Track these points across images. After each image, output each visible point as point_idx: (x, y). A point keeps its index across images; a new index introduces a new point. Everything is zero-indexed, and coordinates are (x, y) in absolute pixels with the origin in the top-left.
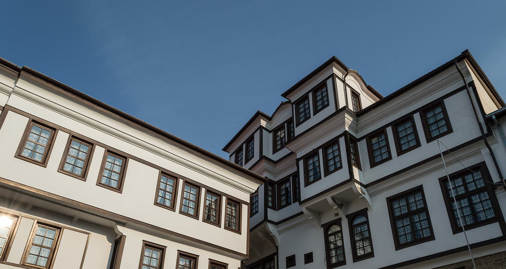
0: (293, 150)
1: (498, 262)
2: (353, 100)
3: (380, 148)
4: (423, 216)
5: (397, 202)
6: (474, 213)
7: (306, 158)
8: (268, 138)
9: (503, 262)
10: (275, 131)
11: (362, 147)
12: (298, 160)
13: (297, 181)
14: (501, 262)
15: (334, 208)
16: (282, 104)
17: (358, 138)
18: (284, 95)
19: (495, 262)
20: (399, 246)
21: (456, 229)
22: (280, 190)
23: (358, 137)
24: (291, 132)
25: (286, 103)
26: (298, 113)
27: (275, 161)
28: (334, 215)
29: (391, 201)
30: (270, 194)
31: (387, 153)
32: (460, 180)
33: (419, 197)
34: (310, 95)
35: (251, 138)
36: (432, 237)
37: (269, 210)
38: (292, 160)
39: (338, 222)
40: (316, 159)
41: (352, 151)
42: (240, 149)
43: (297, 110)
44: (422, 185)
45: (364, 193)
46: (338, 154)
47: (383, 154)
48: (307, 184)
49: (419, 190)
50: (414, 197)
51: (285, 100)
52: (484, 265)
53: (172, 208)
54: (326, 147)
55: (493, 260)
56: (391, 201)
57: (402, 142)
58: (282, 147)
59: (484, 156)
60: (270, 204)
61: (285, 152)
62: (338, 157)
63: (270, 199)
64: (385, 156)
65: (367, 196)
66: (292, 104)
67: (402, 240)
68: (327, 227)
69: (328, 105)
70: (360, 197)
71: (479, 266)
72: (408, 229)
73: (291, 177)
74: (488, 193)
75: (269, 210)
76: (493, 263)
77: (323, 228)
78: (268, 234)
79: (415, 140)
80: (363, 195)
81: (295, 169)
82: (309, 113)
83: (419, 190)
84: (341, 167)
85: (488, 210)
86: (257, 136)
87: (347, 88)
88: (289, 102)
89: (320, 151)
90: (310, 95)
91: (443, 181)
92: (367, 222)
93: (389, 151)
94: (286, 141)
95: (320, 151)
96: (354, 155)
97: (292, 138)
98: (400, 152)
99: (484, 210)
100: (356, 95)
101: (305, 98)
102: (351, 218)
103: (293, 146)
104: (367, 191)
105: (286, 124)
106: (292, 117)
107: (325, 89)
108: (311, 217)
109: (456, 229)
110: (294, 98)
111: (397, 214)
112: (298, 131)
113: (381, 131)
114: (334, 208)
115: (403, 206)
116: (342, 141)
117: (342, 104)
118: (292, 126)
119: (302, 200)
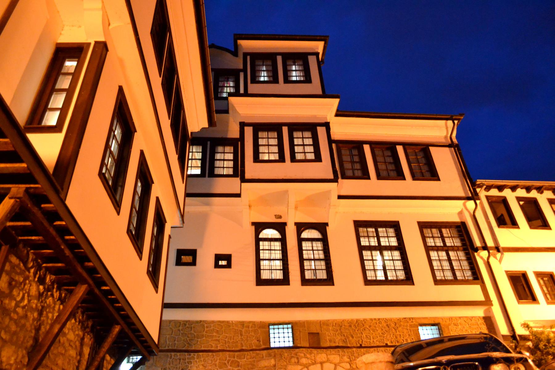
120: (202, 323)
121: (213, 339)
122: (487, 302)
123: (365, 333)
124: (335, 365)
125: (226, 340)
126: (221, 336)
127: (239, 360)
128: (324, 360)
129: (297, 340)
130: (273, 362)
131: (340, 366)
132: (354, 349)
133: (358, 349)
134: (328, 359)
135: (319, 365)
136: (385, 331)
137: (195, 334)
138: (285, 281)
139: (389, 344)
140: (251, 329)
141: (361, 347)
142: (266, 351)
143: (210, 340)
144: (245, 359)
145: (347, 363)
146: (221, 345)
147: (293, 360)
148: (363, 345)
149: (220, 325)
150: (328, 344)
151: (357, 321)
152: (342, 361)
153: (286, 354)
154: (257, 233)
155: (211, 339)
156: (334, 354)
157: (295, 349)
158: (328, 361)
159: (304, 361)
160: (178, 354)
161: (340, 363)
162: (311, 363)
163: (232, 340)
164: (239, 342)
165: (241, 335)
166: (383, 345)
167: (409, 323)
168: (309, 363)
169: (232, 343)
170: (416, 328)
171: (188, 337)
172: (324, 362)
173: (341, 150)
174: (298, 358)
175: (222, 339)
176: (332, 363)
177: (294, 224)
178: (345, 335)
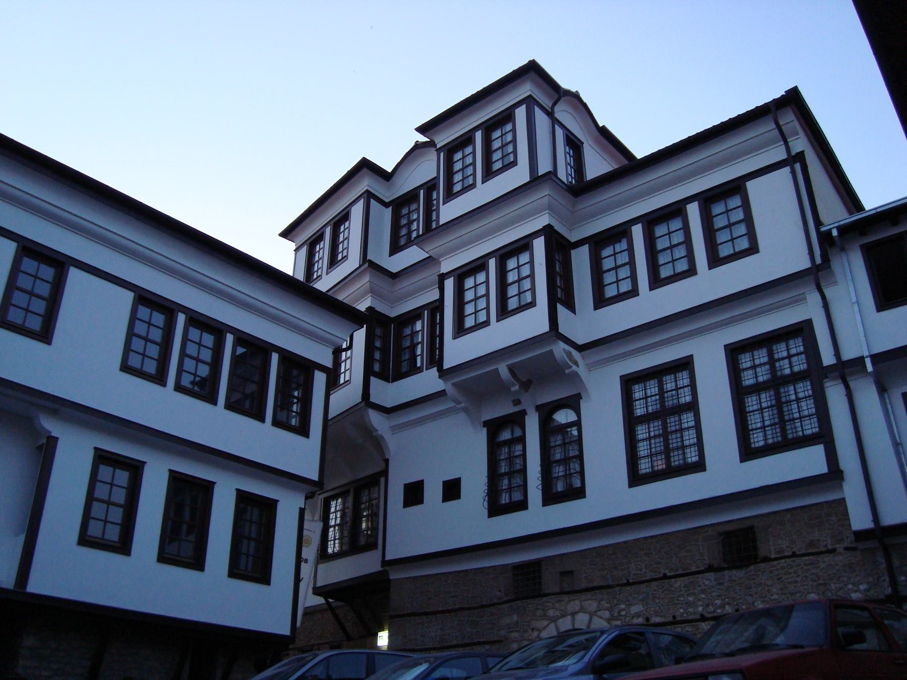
0: (431, 253)
2: (570, 165)
3: (616, 268)
4: (688, 419)
5: (642, 385)
6: (782, 422)
7: (462, 274)
8: (383, 218)
10: (400, 204)
11: (581, 259)
12: (442, 278)
13: (438, 321)
15: (512, 389)
16: (418, 146)
17: (572, 241)
18: (422, 129)
20: (636, 479)
21: (748, 453)
22: (399, 338)
23: (573, 238)
24: (430, 210)
25: (424, 145)
26: (449, 173)
27: (394, 270)
28: (512, 403)
29: (628, 382)
30: (378, 344)
31: (629, 279)
32: (763, 352)
33: (683, 379)
34: (479, 135)
35: (344, 217)
36: (699, 466)
37: (372, 379)
38: (430, 275)
39: (518, 419)
40: (481, 277)
41: (558, 269)
42: (318, 238)
43: (449, 163)
44: (691, 356)
45: (576, 364)
46: (528, 273)
47: (622, 281)
48: (460, 330)
49: (686, 364)
50: (676, 378)
51: (423, 139)
53: (159, 378)
54: (505, 254)
56: (628, 382)
57: (661, 261)
58: (409, 243)
60: (377, 367)
61: (413, 255)
62: (528, 280)
63: (377, 355)
64: (625, 287)
65: (582, 370)
66: (439, 151)
67: (644, 467)
68: (494, 427)
69: (514, 163)
70: (567, 371)
72: (658, 445)
73: (426, 312)
74: (812, 384)
75: (373, 380)
78: (368, 432)
79: (686, 258)
80: (574, 368)
81: (434, 295)
82: (474, 174)
83: (686, 364)
84: (532, 304)
85: (808, 418)
86: (357, 212)
87: (557, 128)
88: (431, 144)
89: (492, 263)
90: (479, 135)
91: (734, 351)
92: (578, 424)
93: (633, 277)
94: (421, 233)
95: (492, 263)
96: (561, 276)
97: (431, 229)
98: (656, 282)
99: (800, 418)
100: (574, 144)
101: (466, 140)
102: (546, 412)
103: (434, 247)
104: (583, 358)
105: (422, 192)
106: (436, 179)
107: (509, 127)
108: (463, 405)
109: (748, 453)
110: (444, 138)
111: (639, 411)
112: (448, 212)
113: (621, 232)
114: (512, 389)
115: (651, 396)
116: (539, 245)
117: (544, 167)
118: (435, 196)
119: (446, 366)
122: (835, 474)
124: (592, 615)
125: (465, 594)
127: (478, 619)
128: (577, 609)
130: (515, 617)
131: (598, 616)
132: (617, 589)
133: (623, 588)
134: (582, 607)
135: (569, 617)
139: (669, 574)
141: (628, 584)
142: (508, 605)
144: (485, 618)
145: (606, 610)
147: (539, 613)
148: (631, 581)
150: (583, 585)
151: (625, 542)
152: (599, 608)
153: (530, 606)
156: (590, 600)
157: (541, 598)
158: (582, 610)
159: (551, 613)
160: (417, 618)
161: (596, 612)
162: (560, 615)
168: (558, 616)
172: (576, 613)
174: (543, 610)
176: (586, 613)
177: (535, 412)
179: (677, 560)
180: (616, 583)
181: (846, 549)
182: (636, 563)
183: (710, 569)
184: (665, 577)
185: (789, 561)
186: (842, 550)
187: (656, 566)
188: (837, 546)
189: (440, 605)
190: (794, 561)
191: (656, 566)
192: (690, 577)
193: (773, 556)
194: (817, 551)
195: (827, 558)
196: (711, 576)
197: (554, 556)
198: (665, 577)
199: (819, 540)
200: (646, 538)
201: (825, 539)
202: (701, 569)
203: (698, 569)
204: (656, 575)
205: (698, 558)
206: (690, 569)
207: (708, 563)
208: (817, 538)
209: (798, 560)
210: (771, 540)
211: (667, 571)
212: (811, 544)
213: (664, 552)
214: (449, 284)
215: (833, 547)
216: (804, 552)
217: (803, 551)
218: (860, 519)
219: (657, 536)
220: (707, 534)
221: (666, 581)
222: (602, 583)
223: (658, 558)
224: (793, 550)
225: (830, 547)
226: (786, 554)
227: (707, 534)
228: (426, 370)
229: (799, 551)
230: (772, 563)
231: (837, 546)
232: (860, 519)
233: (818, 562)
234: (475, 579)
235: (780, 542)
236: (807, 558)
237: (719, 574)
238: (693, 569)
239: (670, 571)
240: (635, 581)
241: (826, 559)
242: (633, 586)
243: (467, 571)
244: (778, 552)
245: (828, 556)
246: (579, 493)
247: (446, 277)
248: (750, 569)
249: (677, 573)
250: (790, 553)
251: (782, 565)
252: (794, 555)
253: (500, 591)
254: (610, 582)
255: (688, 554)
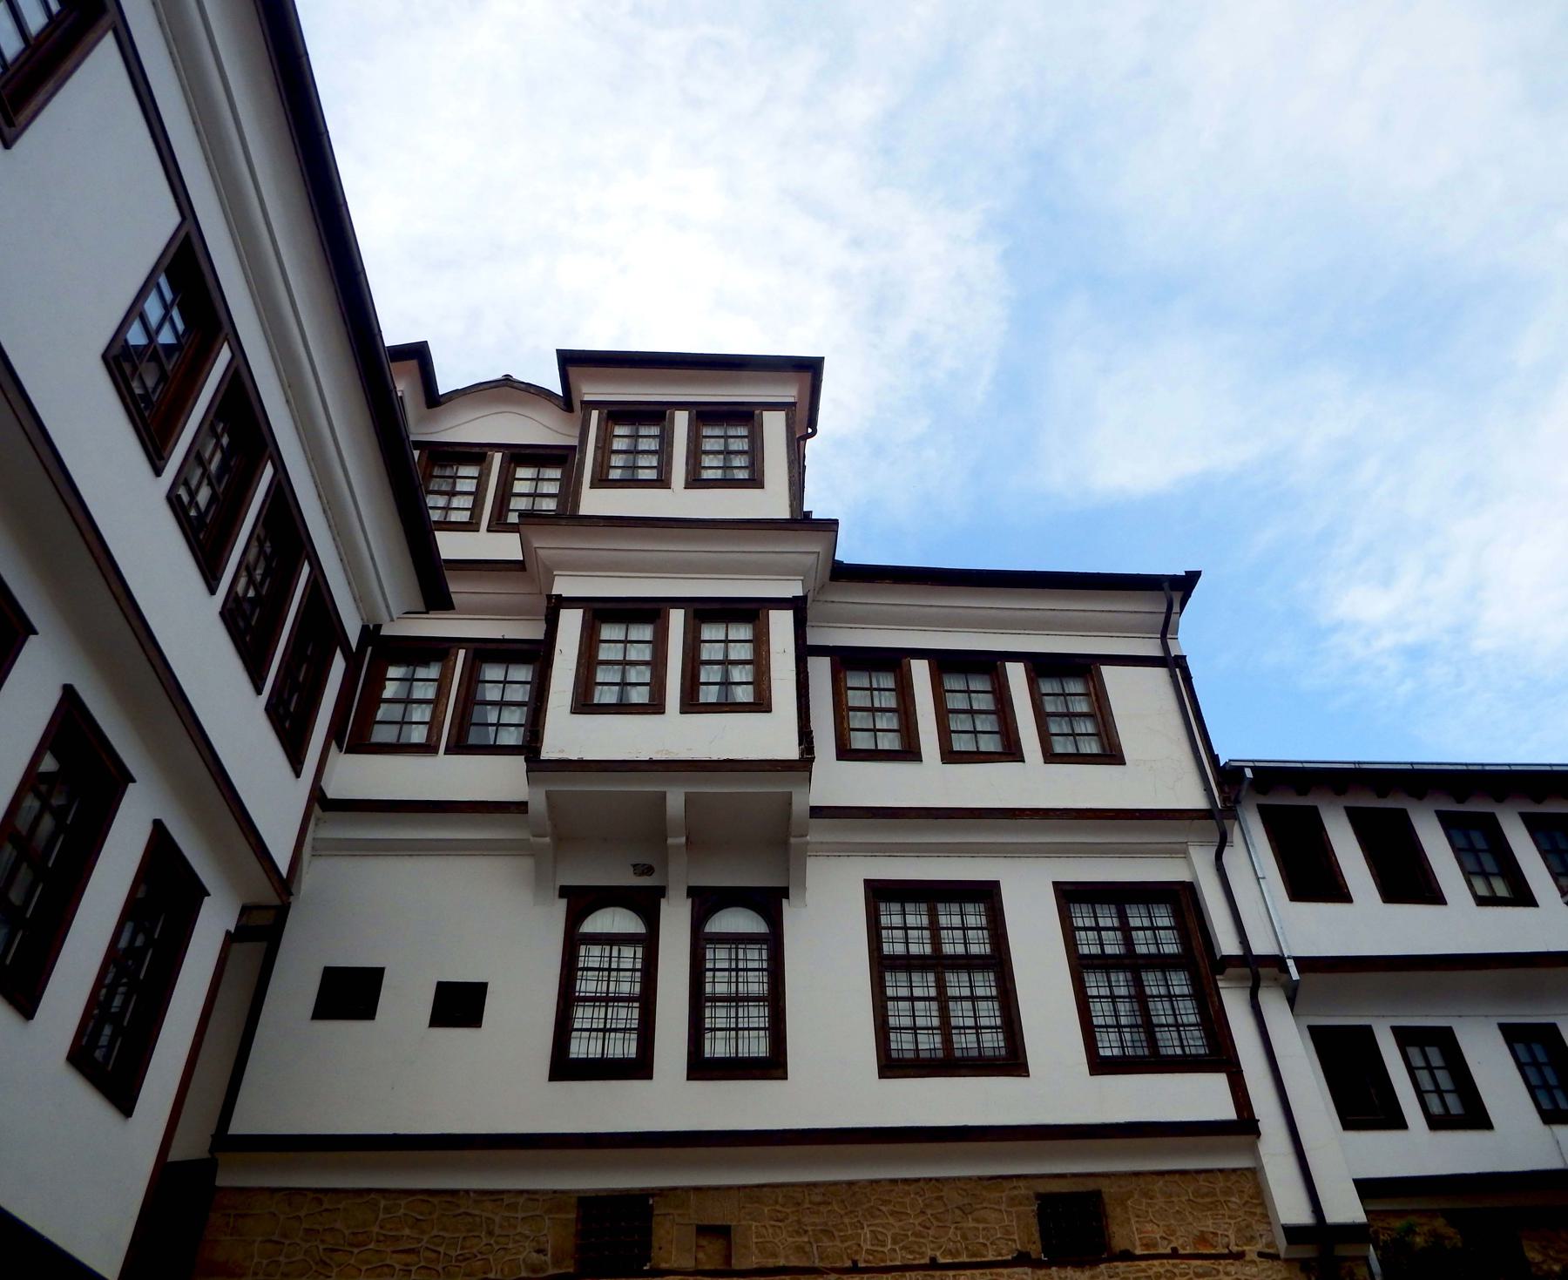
1: (1202, 1198)
9: (1217, 1201)
12: (557, 604)
14: (1212, 1203)
19: (1194, 1197)
52: (1160, 1201)
55: (1190, 1191)
59: (1197, 867)
71: (1144, 1200)
73: (462, 653)
76: (1187, 1198)
77: (690, 900)
120: (372, 1196)
121: (401, 1248)
122: (1245, 1125)
123: (868, 1226)
125: (441, 1249)
126: (426, 1238)
129: (660, 1248)
136: (931, 1218)
137: (347, 1232)
138: (640, 1067)
139: (941, 1260)
140: (523, 1215)
141: (855, 1269)
143: (389, 1250)
146: (423, 1267)
148: (862, 1265)
149: (428, 1201)
151: (851, 1184)
154: (574, 918)
155: (392, 1249)
163: (459, 1252)
164: (479, 1257)
165: (490, 1233)
166: (922, 1262)
167: (1007, 1193)
169: (457, 1261)
170: (1027, 1208)
171: (323, 1241)
173: (868, 671)
175: (427, 1248)
178: (811, 1233)
179: (959, 1233)
180: (829, 1266)
181: (1261, 1255)
182: (873, 1228)
183: (1022, 1259)
184: (933, 1265)
185: (1168, 1264)
186: (1255, 1257)
187: (917, 1240)
188: (1245, 1248)
189: (364, 1268)
190: (1174, 1265)
191: (917, 1240)
192: (988, 1271)
193: (1138, 1252)
194: (1213, 1252)
195: (1233, 1267)
196: (1026, 1274)
197: (687, 1190)
198: (933, 1265)
199: (1215, 1234)
200: (894, 1181)
201: (1226, 1233)
202: (1004, 1258)
203: (1000, 1258)
204: (914, 1259)
205: (999, 1236)
206: (984, 1257)
207: (1019, 1247)
208: (1212, 1230)
209: (1183, 1265)
210: (1133, 1222)
211: (938, 1254)
212: (1202, 1239)
213: (932, 1215)
214: (571, 623)
215: (1240, 1249)
216: (1192, 1252)
217: (1188, 1251)
218: (1291, 1208)
219: (917, 1180)
220: (1016, 1192)
221: (938, 1273)
222: (795, 1262)
223: (920, 1224)
224: (1173, 1245)
225: (1235, 1249)
226: (1161, 1251)
227: (1016, 1192)
228: (447, 752)
229: (1184, 1249)
230: (1137, 1263)
231: (1245, 1248)
232: (1291, 1208)
233: (1218, 1272)
234: (476, 1215)
235: (1149, 1227)
236: (1199, 1262)
237: (1041, 1273)
238: (990, 1258)
239: (944, 1255)
240: (869, 1265)
241: (1232, 1269)
242: (866, 1276)
243: (454, 1193)
244: (1147, 1246)
245: (1232, 1264)
246: (773, 1066)
247: (564, 604)
248: (1099, 1270)
249: (956, 1260)
250: (1168, 1251)
251: (1155, 1269)
252: (1175, 1254)
253: (539, 1251)
254: (817, 1261)
255: (981, 1226)
